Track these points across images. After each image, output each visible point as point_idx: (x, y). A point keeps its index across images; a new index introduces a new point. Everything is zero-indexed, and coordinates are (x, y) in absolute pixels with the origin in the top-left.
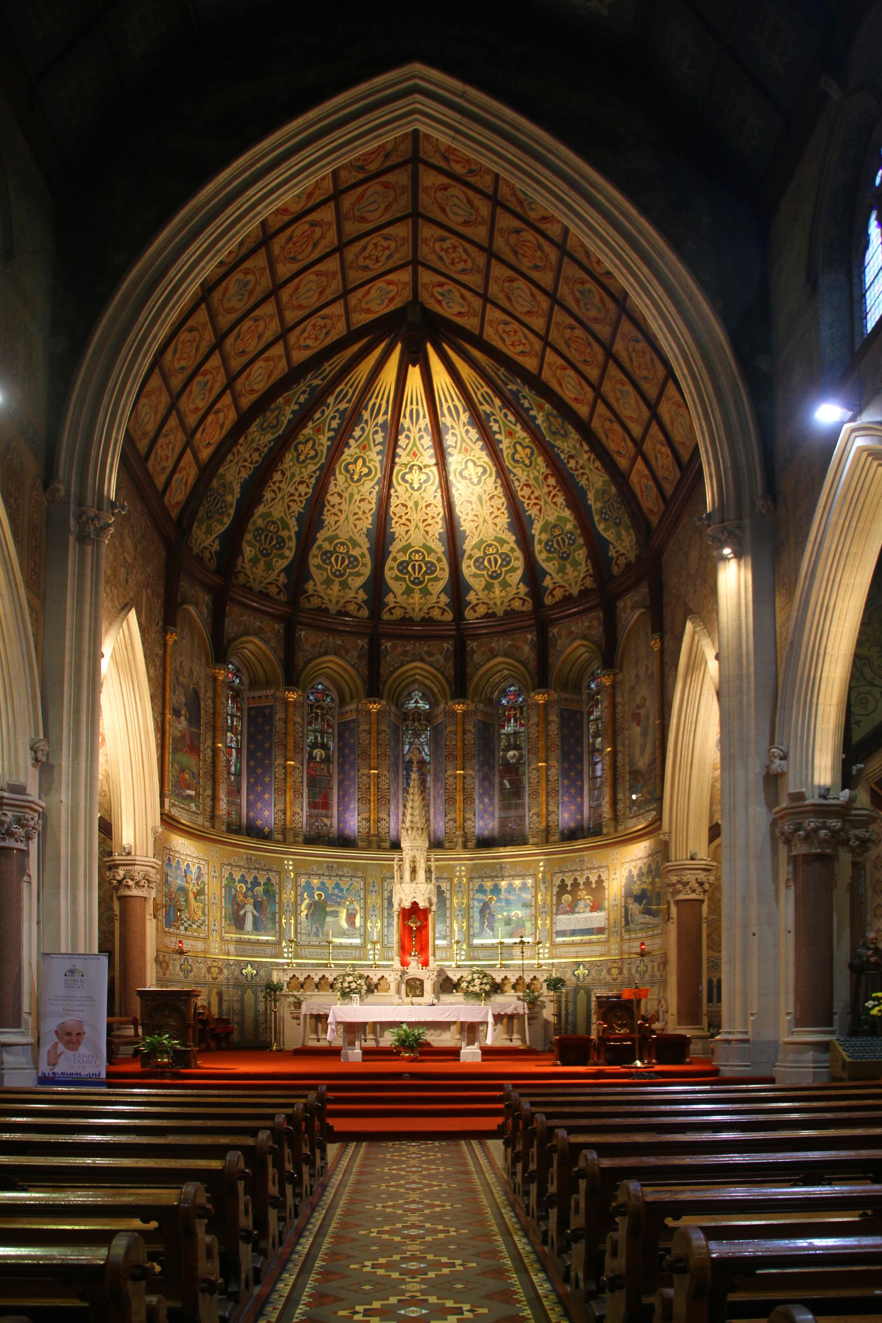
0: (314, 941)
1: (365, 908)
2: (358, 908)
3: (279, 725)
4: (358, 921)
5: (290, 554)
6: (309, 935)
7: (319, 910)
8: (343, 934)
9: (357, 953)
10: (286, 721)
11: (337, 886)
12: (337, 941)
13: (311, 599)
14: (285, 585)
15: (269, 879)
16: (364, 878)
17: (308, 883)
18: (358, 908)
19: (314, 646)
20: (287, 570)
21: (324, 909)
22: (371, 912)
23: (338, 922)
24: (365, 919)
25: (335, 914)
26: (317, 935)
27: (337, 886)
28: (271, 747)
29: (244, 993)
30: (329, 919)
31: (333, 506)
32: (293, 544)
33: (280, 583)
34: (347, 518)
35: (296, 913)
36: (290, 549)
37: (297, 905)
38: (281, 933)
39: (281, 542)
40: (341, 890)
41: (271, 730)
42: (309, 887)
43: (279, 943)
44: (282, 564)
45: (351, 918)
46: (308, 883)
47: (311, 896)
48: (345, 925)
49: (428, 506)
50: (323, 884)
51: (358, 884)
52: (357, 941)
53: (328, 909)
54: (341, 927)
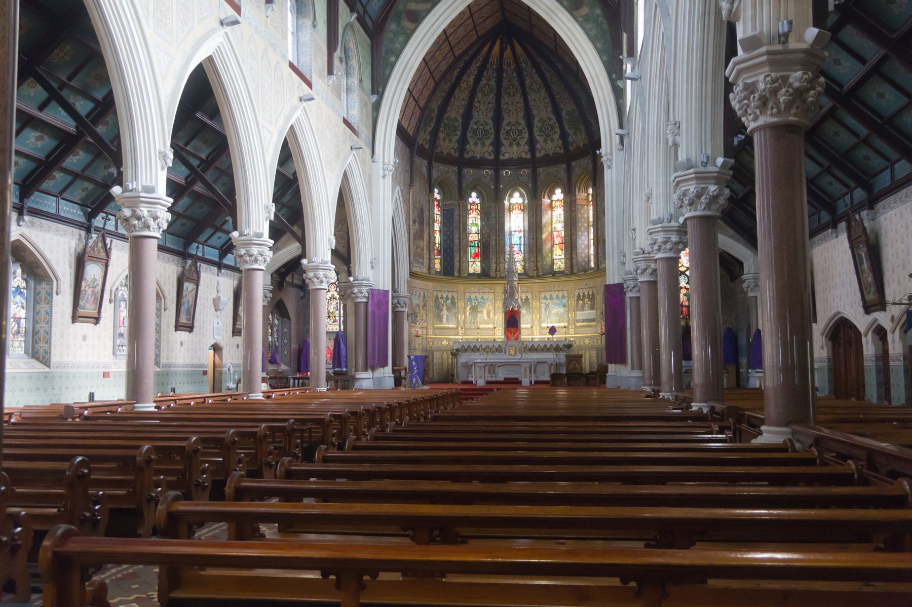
0: (473, 326)
1: (494, 308)
2: (491, 309)
3: (456, 218)
4: (492, 315)
5: (459, 133)
6: (470, 323)
7: (474, 309)
8: (485, 322)
9: (491, 332)
10: (459, 215)
11: (482, 297)
12: (482, 326)
13: (469, 153)
14: (458, 148)
15: (453, 296)
16: (494, 293)
17: (470, 297)
18: (491, 309)
19: (470, 176)
20: (458, 141)
21: (477, 310)
22: (497, 311)
23: (483, 316)
24: (495, 314)
25: (481, 312)
26: (474, 323)
27: (482, 297)
28: (453, 230)
29: (443, 354)
30: (479, 315)
31: (477, 108)
32: (460, 128)
33: (455, 147)
34: (483, 113)
35: (465, 313)
36: (459, 130)
37: (465, 308)
38: (458, 323)
39: (455, 128)
40: (484, 300)
41: (453, 221)
42: (470, 299)
43: (457, 328)
44: (455, 138)
45: (488, 314)
46: (470, 297)
47: (471, 304)
48: (486, 318)
49: (518, 103)
50: (476, 297)
51: (491, 296)
52: (491, 326)
53: (479, 310)
54: (484, 319)
